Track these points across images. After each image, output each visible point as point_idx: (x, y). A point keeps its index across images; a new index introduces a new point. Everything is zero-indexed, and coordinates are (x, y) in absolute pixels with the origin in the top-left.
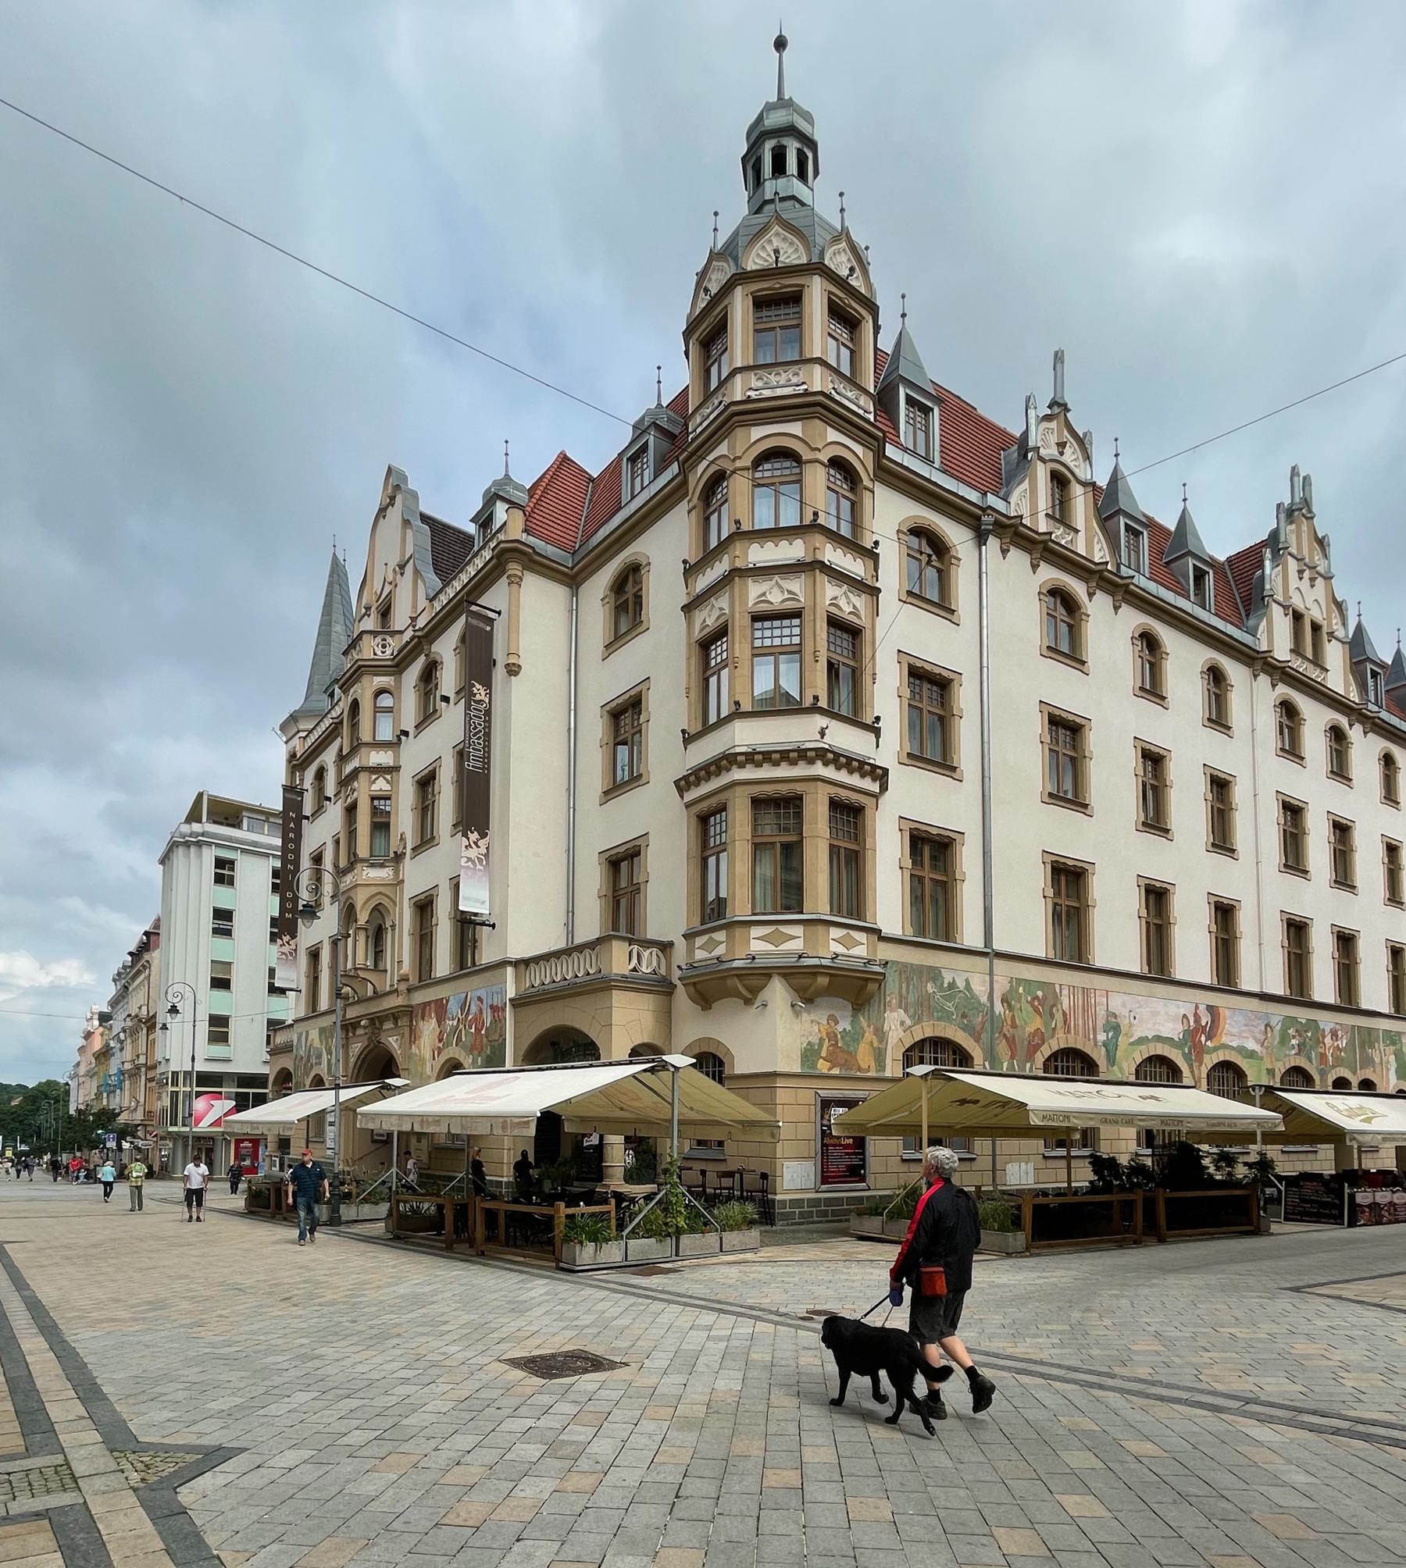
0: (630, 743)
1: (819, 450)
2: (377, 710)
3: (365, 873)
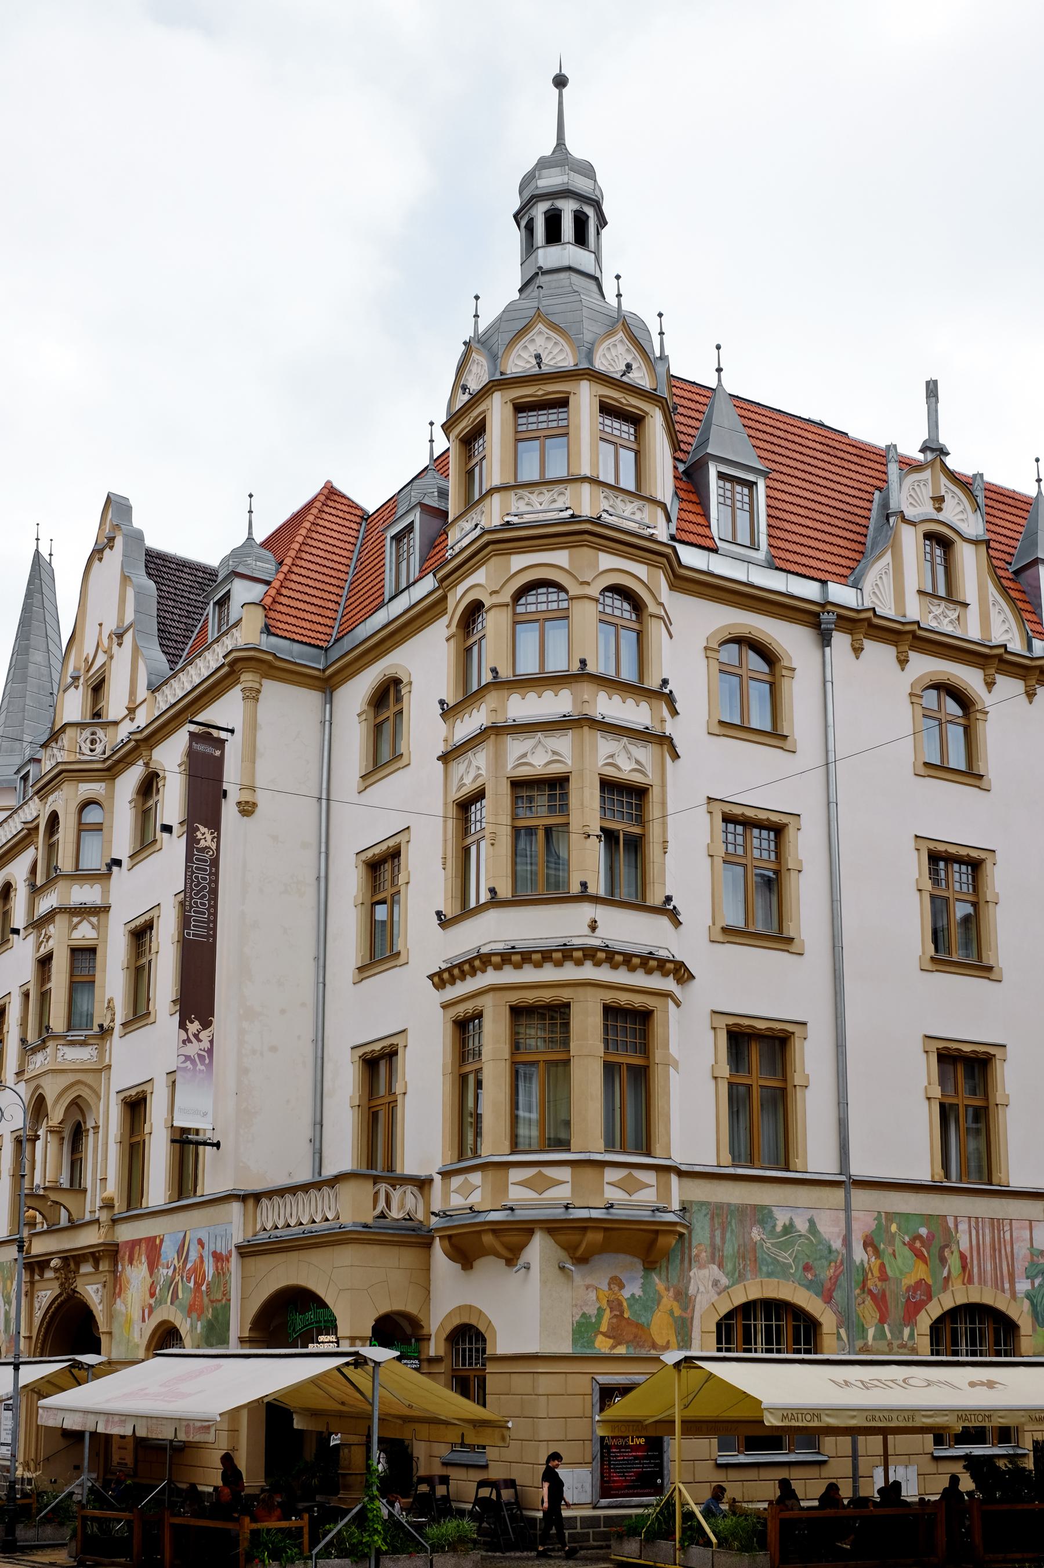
0: (389, 901)
1: (588, 584)
2: (82, 828)
3: (60, 1054)
